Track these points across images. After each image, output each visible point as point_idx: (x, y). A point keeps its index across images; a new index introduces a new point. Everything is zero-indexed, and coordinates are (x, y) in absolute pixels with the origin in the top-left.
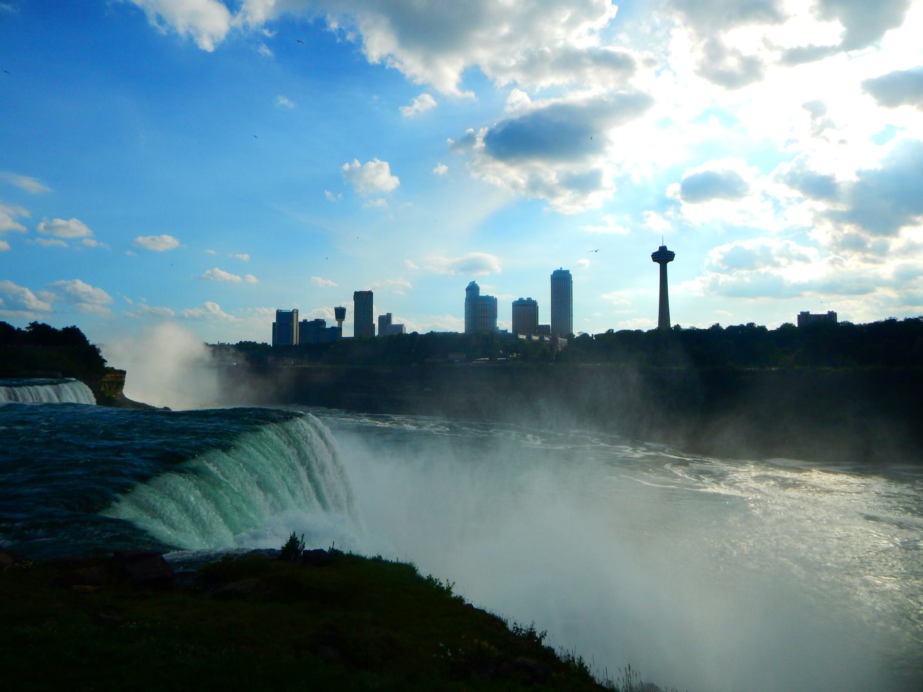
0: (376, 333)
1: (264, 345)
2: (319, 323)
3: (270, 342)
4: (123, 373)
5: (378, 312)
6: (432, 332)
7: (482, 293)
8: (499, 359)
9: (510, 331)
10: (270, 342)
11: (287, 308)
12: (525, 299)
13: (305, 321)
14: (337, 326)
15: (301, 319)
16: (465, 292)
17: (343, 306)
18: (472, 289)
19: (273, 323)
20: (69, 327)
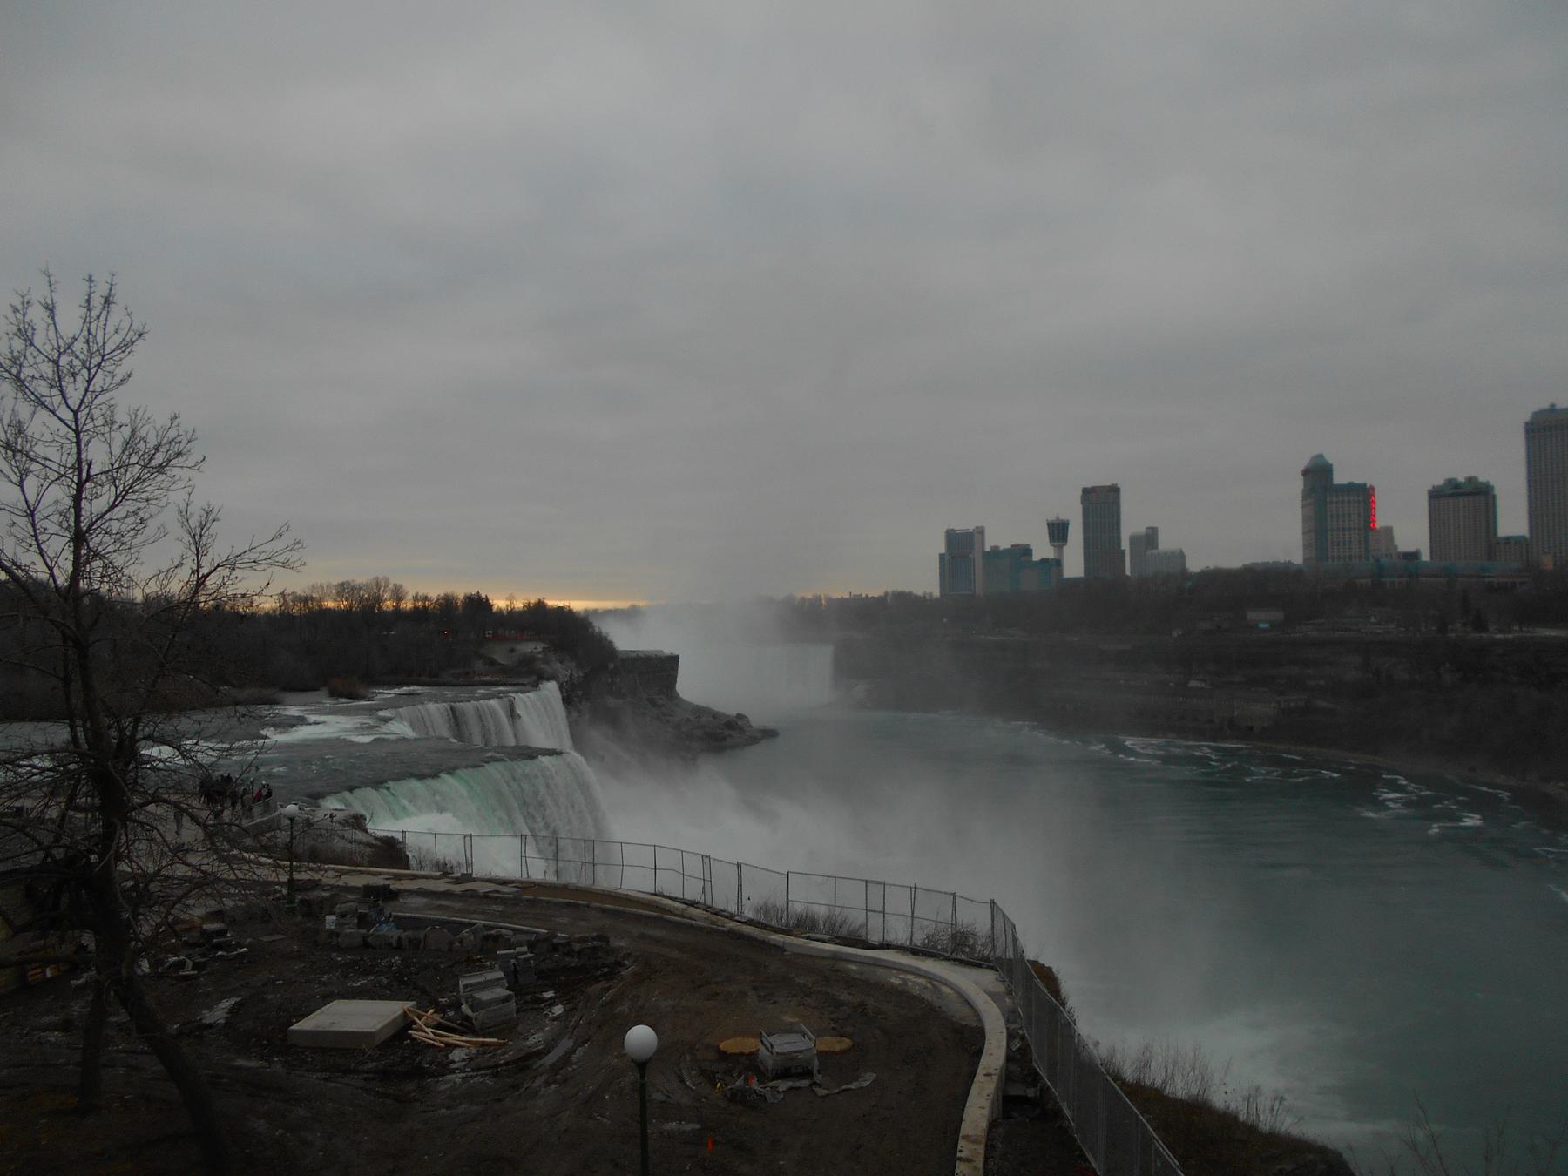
4: (674, 660)
5: (1131, 523)
7: (1339, 478)
10: (937, 593)
11: (964, 524)
12: (1461, 479)
13: (995, 550)
15: (988, 548)
16: (1302, 477)
17: (1063, 517)
18: (1318, 475)
19: (941, 555)
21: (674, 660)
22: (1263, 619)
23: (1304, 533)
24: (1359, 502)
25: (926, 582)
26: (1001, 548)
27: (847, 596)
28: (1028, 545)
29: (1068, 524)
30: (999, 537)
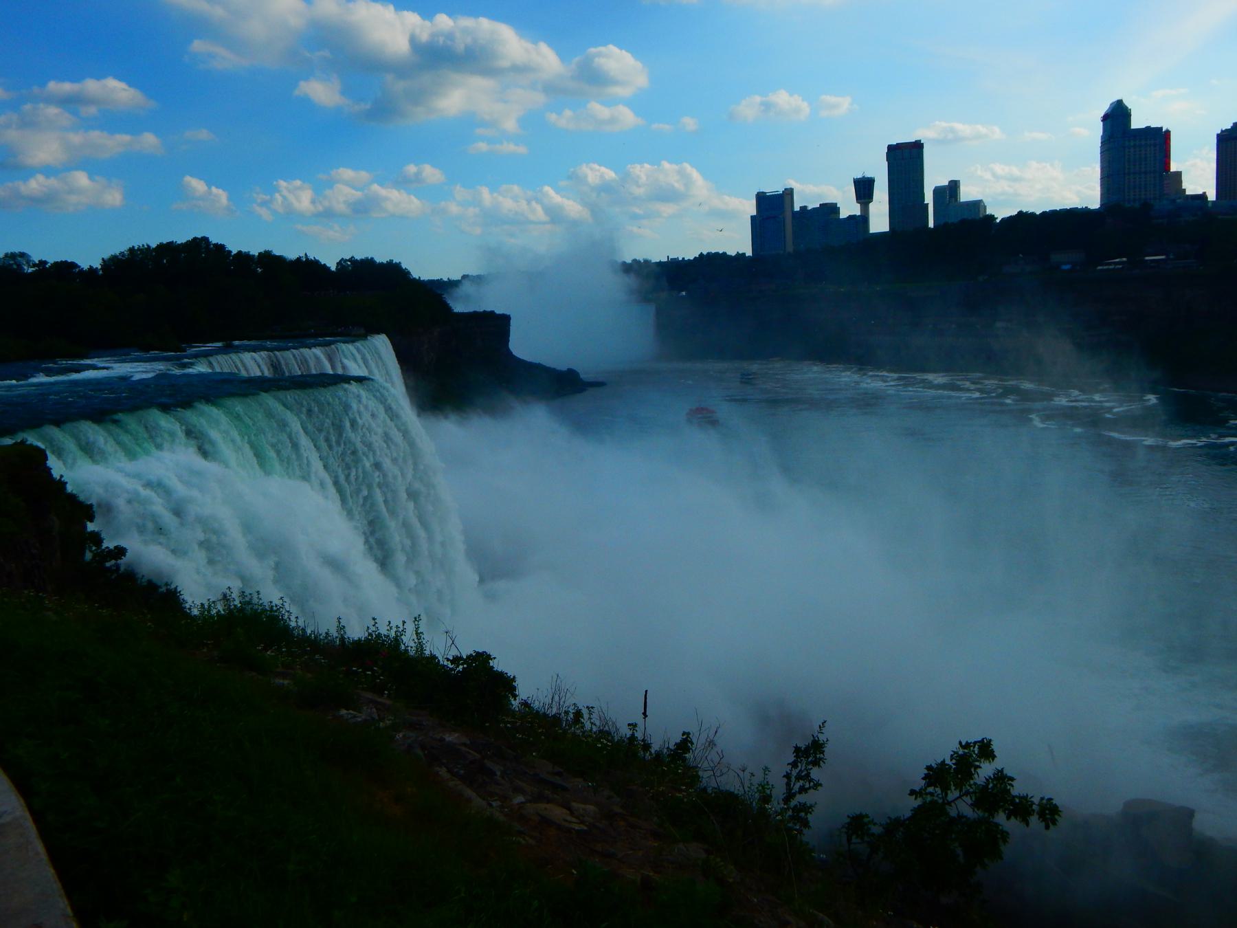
0: (931, 224)
1: (740, 257)
2: (830, 209)
3: (749, 253)
4: (505, 320)
5: (934, 178)
6: (1020, 213)
7: (1137, 123)
8: (1147, 258)
9: (1212, 196)
10: (749, 253)
11: (773, 187)
13: (803, 209)
14: (858, 213)
15: (797, 208)
16: (1102, 123)
17: (868, 175)
18: (1117, 116)
19: (751, 217)
20: (378, 259)
21: (505, 320)
22: (1065, 261)
23: (1101, 179)
24: (1155, 145)
25: (738, 242)
26: (809, 208)
27: (666, 260)
28: (836, 204)
29: (874, 181)
30: (808, 196)
